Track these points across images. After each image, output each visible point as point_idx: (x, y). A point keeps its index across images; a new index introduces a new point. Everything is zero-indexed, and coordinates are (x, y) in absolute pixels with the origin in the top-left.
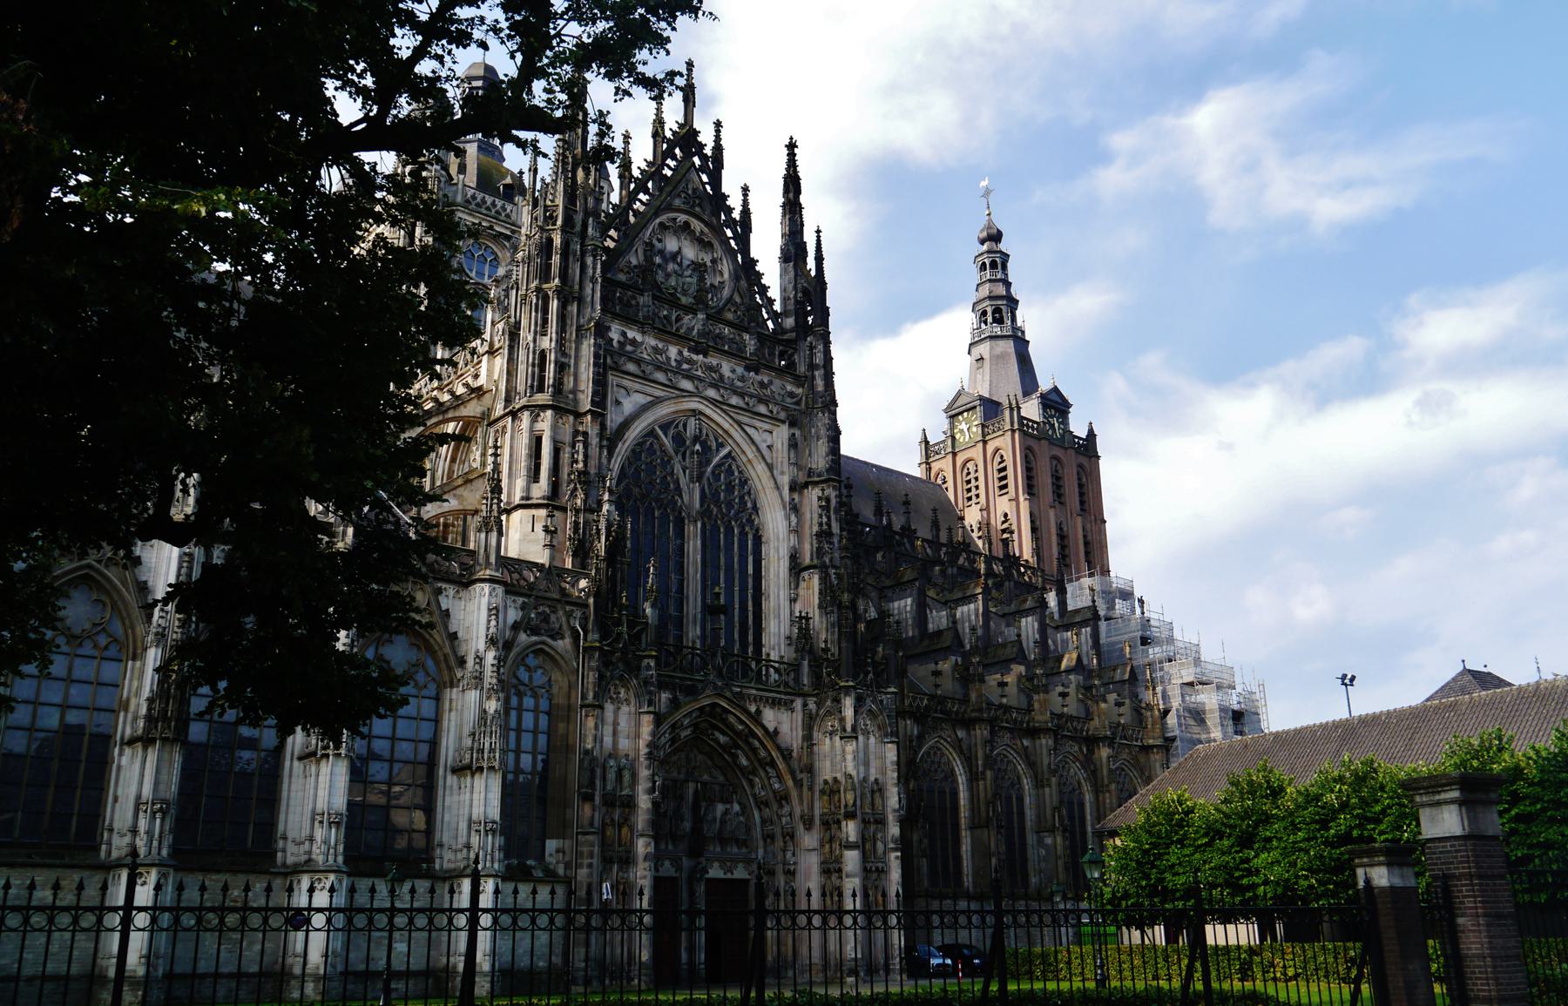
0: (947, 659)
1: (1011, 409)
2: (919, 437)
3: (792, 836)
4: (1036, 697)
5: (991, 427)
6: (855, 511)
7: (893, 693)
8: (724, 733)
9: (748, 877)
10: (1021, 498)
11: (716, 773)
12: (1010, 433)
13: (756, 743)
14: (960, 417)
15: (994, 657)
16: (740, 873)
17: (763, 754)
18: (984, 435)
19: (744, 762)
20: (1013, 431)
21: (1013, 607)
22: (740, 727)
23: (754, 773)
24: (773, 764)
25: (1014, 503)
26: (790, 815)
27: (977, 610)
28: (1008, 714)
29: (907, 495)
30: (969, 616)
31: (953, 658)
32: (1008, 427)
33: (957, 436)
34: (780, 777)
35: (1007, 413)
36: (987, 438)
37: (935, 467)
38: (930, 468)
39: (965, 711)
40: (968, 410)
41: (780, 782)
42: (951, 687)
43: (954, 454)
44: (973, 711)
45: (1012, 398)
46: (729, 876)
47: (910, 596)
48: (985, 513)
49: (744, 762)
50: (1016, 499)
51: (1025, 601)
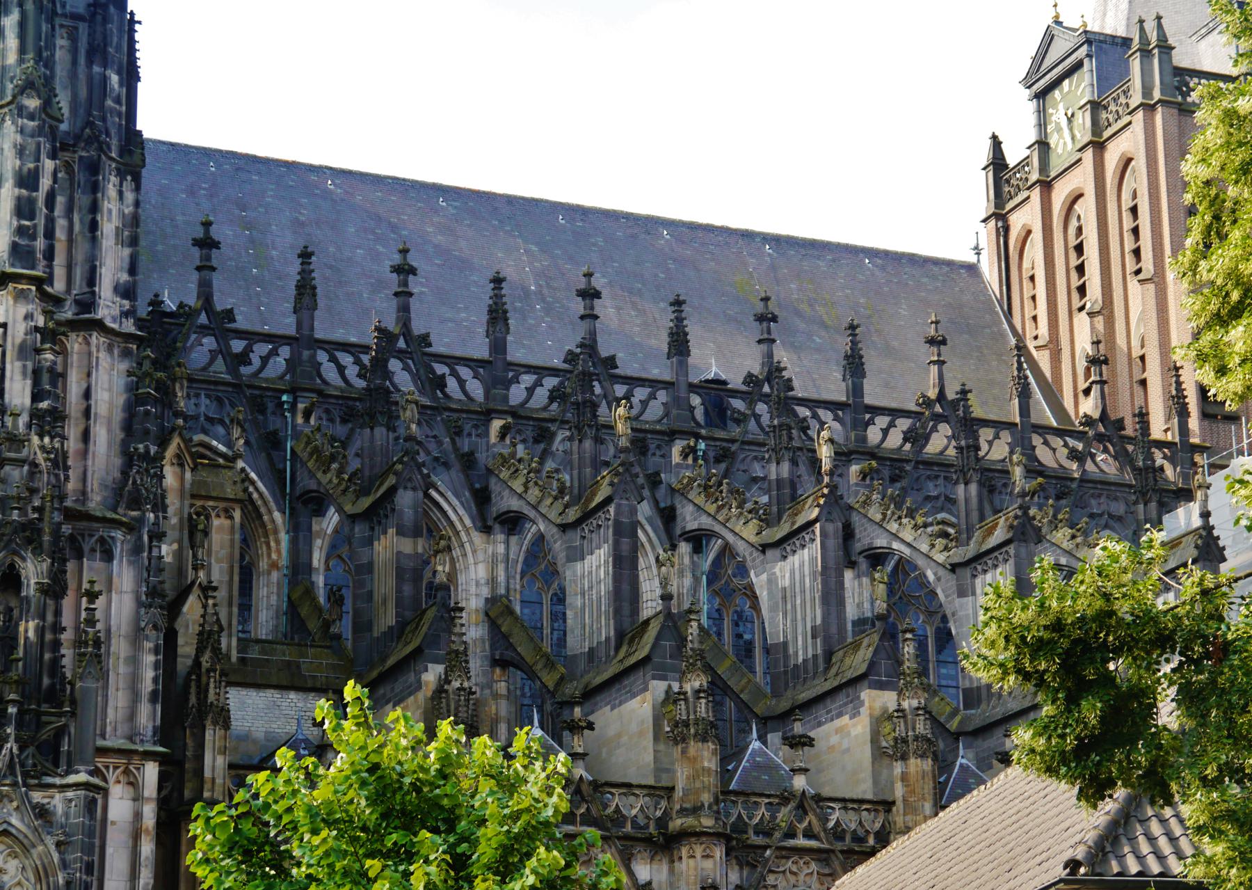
0: (646, 689)
1: (1146, 53)
2: (983, 154)
4: (898, 768)
5: (1112, 107)
6: (604, 352)
7: (77, 786)
10: (1170, 276)
12: (1140, 115)
14: (1057, 93)
15: (837, 674)
18: (1097, 128)
20: (1149, 108)
21: (971, 550)
25: (1151, 287)
27: (813, 560)
28: (811, 817)
29: (766, 299)
30: (803, 577)
31: (658, 688)
32: (1136, 99)
33: (1052, 141)
35: (1136, 65)
36: (1106, 134)
37: (1017, 221)
38: (1007, 229)
39: (667, 815)
40: (1068, 73)
42: (649, 757)
43: (1046, 186)
44: (683, 812)
45: (1150, 26)
47: (606, 541)
48: (1100, 322)
50: (1158, 280)
51: (990, 532)
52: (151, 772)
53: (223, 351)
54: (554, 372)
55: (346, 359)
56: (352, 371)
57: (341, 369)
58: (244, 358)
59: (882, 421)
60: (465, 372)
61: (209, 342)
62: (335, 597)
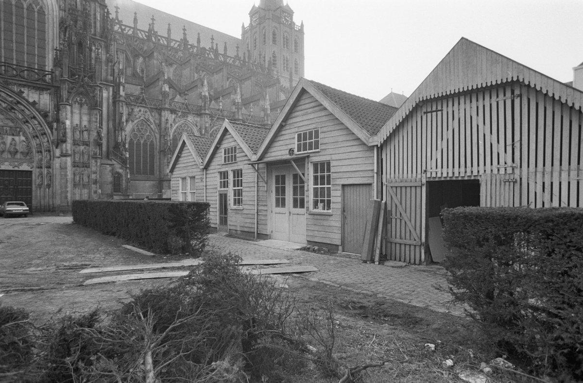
3: (49, 151)
8: (5, 103)
9: (30, 170)
11: (7, 122)
13: (23, 108)
16: (25, 167)
17: (27, 112)
19: (20, 116)
22: (10, 99)
23: (27, 122)
24: (34, 117)
26: (48, 141)
34: (39, 123)
41: (42, 127)
46: (16, 169)
49: (20, 116)
52: (111, 89)
53: (120, 27)
54: (178, 41)
55: (143, 33)
56: (144, 36)
57: (142, 35)
58: (124, 29)
59: (229, 58)
60: (164, 39)
61: (118, 26)
62: (142, 71)
